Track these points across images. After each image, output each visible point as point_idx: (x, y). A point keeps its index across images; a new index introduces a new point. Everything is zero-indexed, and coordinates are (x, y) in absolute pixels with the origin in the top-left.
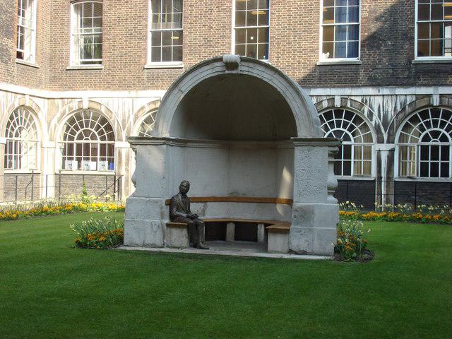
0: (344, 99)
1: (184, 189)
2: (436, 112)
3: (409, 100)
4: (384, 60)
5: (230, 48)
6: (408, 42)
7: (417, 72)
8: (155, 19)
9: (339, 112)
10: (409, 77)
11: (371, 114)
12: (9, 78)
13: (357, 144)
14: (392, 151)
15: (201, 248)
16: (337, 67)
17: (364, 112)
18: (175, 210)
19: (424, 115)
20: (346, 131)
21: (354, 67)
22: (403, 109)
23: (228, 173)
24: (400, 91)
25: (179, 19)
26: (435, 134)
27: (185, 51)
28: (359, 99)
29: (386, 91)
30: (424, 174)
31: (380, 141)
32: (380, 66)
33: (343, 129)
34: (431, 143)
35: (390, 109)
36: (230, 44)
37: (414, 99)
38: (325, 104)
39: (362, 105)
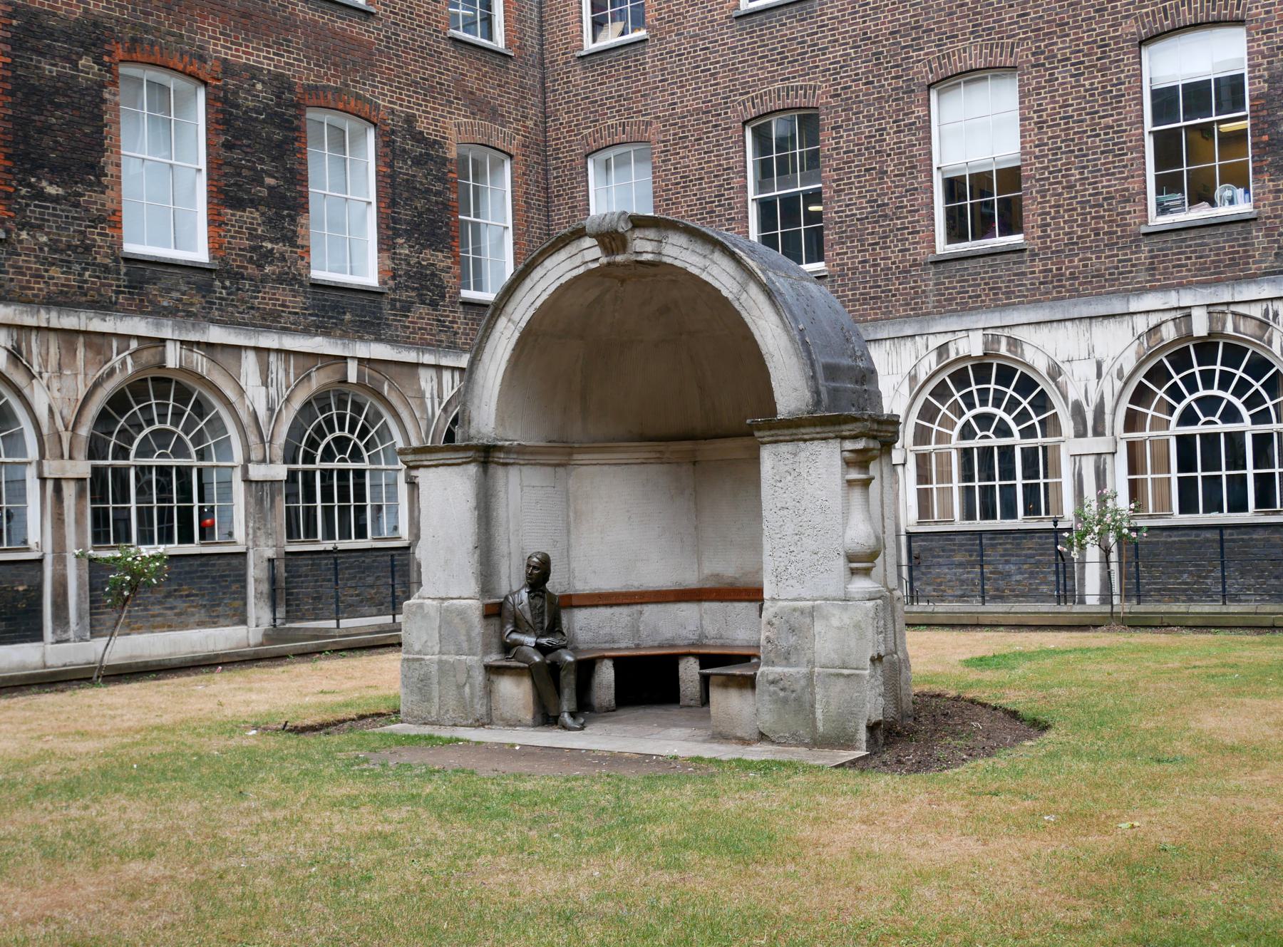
1: (538, 574)
5: (931, 218)
8: (765, 170)
9: (1206, 349)
12: (443, 337)
13: (1030, 442)
15: (565, 727)
16: (1193, 234)
17: (1270, 342)
18: (509, 628)
21: (1239, 228)
23: (696, 528)
25: (813, 160)
27: (829, 236)
28: (1256, 311)
30: (1187, 505)
36: (930, 205)
38: (1169, 333)
39: (1264, 325)
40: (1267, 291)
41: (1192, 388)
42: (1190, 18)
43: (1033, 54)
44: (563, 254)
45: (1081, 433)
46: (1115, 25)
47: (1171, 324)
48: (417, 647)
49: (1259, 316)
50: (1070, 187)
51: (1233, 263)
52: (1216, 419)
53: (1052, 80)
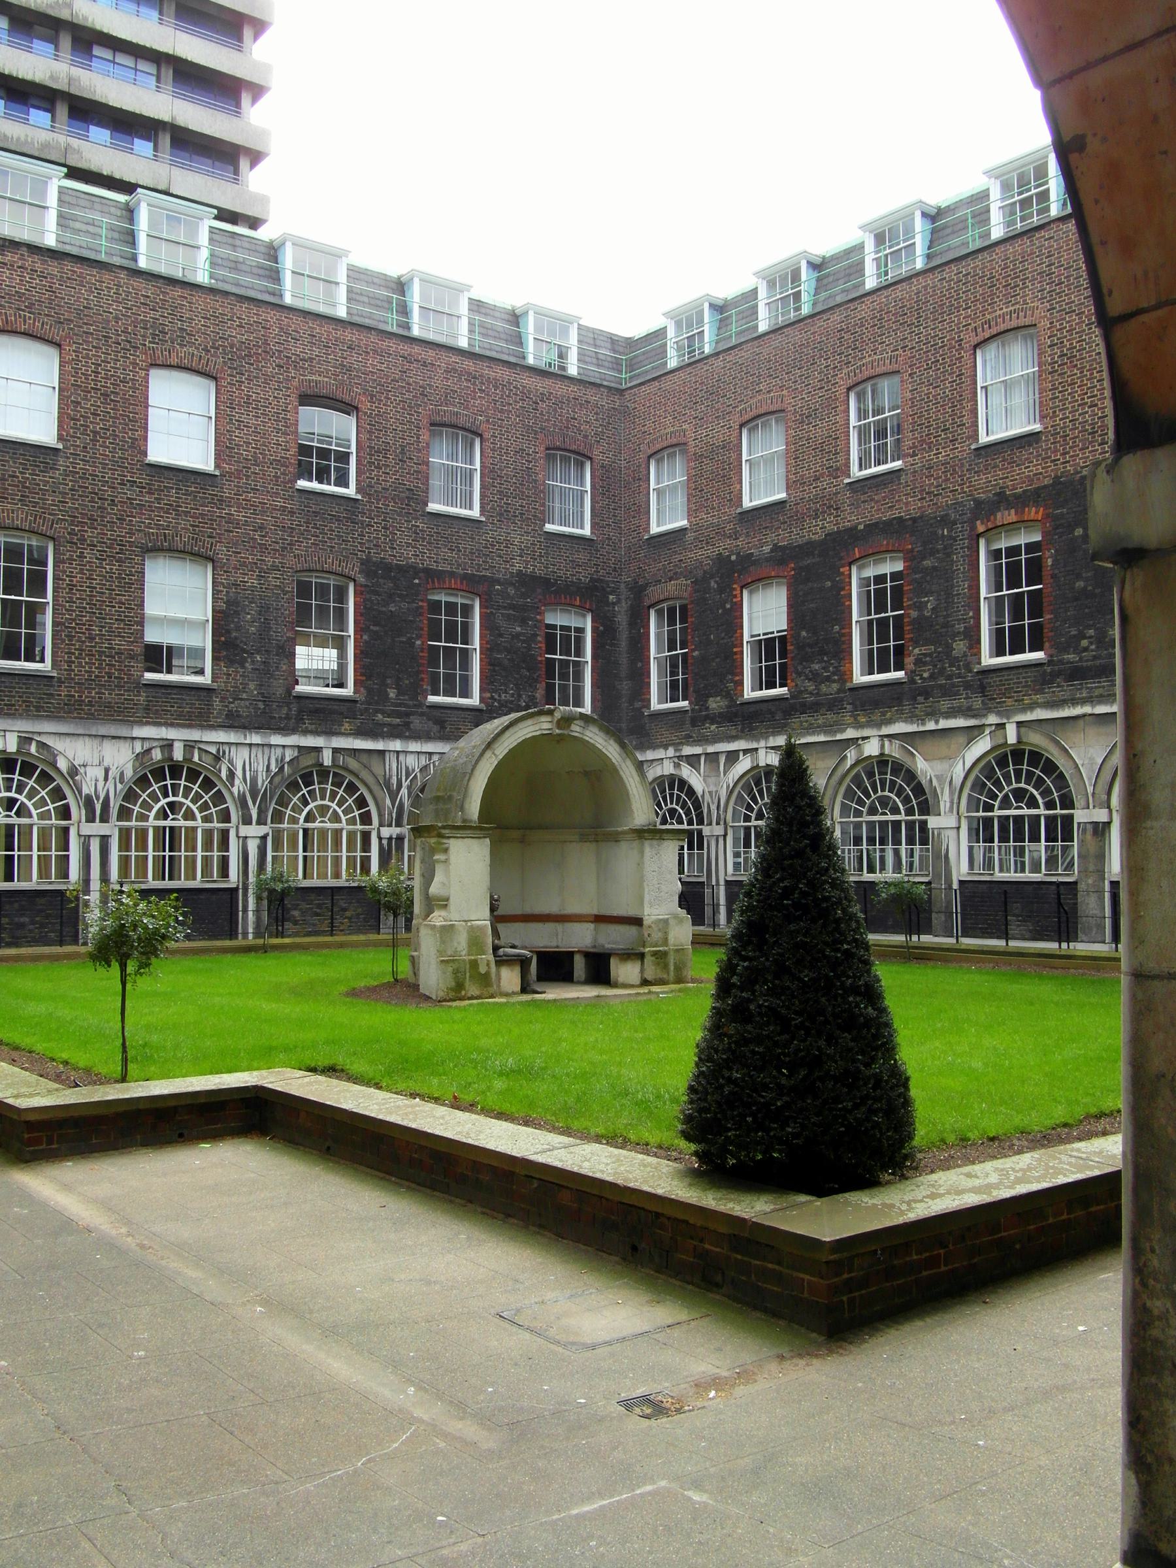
0: (189, 746)
2: (324, 773)
3: (289, 755)
4: (252, 686)
6: (286, 661)
7: (300, 711)
10: (288, 717)
11: (231, 775)
14: (264, 838)
17: (220, 771)
19: (308, 780)
20: (188, 802)
22: (281, 769)
24: (276, 739)
26: (323, 810)
28: (213, 750)
29: (256, 739)
31: (247, 821)
32: (244, 696)
33: (183, 800)
34: (316, 824)
35: (260, 769)
37: (296, 754)
38: (157, 755)
39: (217, 758)
40: (221, 736)
41: (340, 805)
42: (181, 546)
43: (69, 533)
44: (529, 722)
45: (91, 819)
46: (131, 533)
47: (158, 750)
48: (449, 953)
49: (214, 752)
50: (91, 639)
51: (200, 715)
52: (179, 817)
53: (82, 556)
